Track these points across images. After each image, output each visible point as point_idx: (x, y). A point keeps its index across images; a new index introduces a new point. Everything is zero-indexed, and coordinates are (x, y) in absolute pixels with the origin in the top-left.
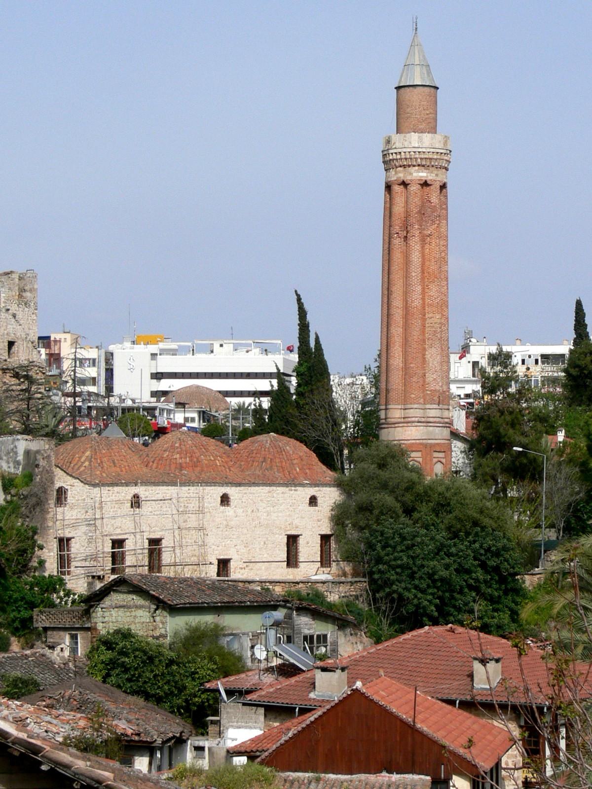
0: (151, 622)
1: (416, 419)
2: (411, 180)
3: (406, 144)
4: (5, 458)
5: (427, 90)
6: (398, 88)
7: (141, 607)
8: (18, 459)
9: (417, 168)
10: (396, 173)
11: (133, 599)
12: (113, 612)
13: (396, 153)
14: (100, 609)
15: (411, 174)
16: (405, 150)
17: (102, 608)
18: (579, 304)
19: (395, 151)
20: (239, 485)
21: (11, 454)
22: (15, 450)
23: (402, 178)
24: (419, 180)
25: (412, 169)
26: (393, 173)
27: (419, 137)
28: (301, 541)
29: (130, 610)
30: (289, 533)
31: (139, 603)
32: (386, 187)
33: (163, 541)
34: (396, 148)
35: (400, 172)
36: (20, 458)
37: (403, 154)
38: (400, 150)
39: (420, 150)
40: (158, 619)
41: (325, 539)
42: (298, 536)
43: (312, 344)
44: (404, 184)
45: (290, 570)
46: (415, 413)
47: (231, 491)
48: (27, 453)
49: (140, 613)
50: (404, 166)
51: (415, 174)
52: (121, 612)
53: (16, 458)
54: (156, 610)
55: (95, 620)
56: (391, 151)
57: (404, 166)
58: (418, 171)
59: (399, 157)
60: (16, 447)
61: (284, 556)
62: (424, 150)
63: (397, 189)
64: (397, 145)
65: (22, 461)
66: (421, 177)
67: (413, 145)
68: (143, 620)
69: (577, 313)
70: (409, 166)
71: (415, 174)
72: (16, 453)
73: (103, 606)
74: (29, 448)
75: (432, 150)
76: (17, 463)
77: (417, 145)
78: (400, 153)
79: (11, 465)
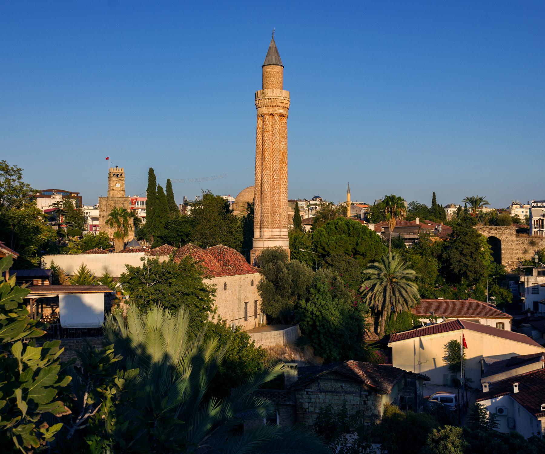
0: (362, 405)
1: (278, 237)
2: (276, 114)
3: (274, 94)
6: (262, 67)
7: (351, 393)
9: (278, 107)
10: (267, 109)
11: (342, 387)
12: (319, 396)
13: (268, 99)
14: (305, 393)
15: (276, 110)
16: (273, 97)
17: (307, 393)
24: (280, 114)
25: (276, 108)
26: (266, 109)
27: (280, 91)
29: (339, 394)
30: (245, 302)
31: (349, 389)
34: (268, 96)
37: (272, 99)
38: (271, 97)
39: (279, 98)
41: (256, 302)
42: (248, 302)
44: (272, 115)
45: (246, 322)
46: (267, 234)
49: (350, 397)
50: (273, 106)
51: (278, 111)
52: (329, 396)
54: (366, 396)
55: (300, 400)
57: (273, 106)
58: (279, 109)
61: (243, 315)
62: (282, 98)
63: (267, 117)
64: (269, 95)
66: (280, 112)
67: (278, 95)
68: (353, 403)
70: (275, 106)
71: (278, 111)
73: (309, 390)
75: (286, 99)
77: (279, 96)
78: (271, 99)
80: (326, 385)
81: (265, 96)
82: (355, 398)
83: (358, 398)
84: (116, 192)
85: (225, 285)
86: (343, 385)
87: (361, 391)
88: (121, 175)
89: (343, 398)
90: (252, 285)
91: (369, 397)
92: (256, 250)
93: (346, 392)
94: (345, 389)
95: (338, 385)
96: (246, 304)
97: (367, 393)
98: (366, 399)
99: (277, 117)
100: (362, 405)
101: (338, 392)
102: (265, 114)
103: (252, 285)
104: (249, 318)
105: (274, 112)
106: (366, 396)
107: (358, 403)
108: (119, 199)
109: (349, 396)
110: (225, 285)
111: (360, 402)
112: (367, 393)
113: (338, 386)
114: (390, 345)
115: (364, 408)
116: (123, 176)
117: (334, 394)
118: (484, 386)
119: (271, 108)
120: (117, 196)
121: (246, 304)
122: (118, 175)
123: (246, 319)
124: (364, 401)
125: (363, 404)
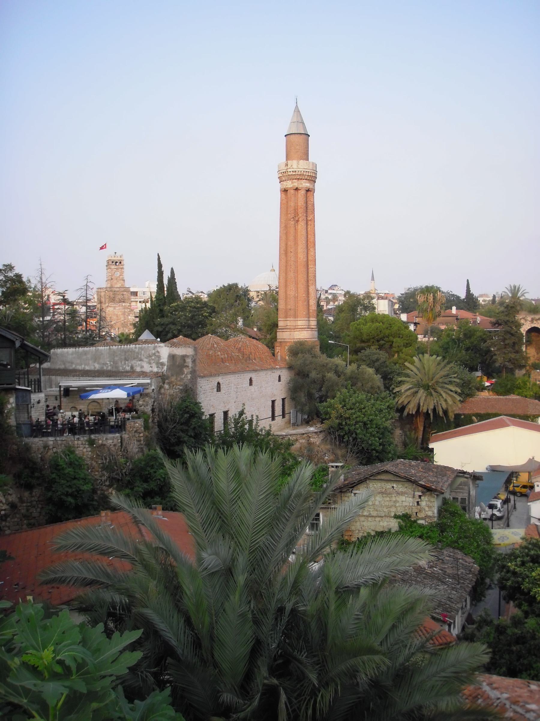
3: (300, 166)
4: (146, 360)
5: (303, 136)
7: (402, 494)
8: (161, 361)
9: (305, 181)
10: (292, 183)
11: (393, 487)
15: (302, 184)
16: (299, 170)
18: (172, 269)
19: (293, 170)
20: (255, 371)
21: (153, 357)
22: (157, 354)
23: (296, 186)
28: (276, 404)
31: (400, 490)
32: (281, 191)
33: (229, 412)
35: (295, 182)
36: (164, 359)
40: (423, 504)
41: (283, 400)
43: (165, 282)
44: (297, 189)
45: (273, 422)
47: (253, 375)
48: (172, 357)
53: (159, 360)
54: (420, 496)
56: (289, 170)
57: (298, 179)
59: (294, 173)
60: (158, 352)
61: (270, 415)
65: (166, 363)
68: (405, 504)
69: (171, 273)
70: (301, 179)
72: (159, 357)
74: (173, 353)
75: (313, 171)
76: (162, 364)
77: (305, 168)
79: (154, 365)
80: (375, 486)
81: (290, 168)
82: (407, 499)
83: (411, 499)
84: (115, 281)
85: (251, 380)
86: (395, 486)
87: (414, 492)
88: (120, 263)
89: (394, 499)
90: (279, 380)
91: (422, 498)
92: (281, 342)
93: (398, 493)
94: (397, 490)
95: (389, 486)
96: (273, 402)
97: (420, 494)
98: (420, 500)
99: (302, 192)
100: (415, 506)
101: (390, 494)
102: (291, 188)
103: (279, 380)
104: (276, 418)
105: (300, 186)
106: (420, 496)
107: (411, 505)
108: (118, 289)
109: (401, 497)
110: (251, 380)
111: (413, 503)
112: (420, 494)
113: (388, 487)
114: (431, 446)
115: (417, 509)
116: (122, 263)
117: (384, 495)
118: (536, 486)
119: (296, 181)
120: (116, 286)
121: (273, 402)
122: (116, 262)
123: (273, 418)
124: (418, 502)
125: (416, 505)
